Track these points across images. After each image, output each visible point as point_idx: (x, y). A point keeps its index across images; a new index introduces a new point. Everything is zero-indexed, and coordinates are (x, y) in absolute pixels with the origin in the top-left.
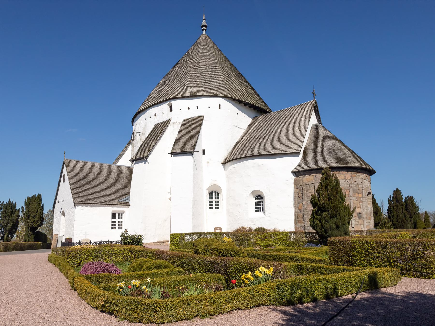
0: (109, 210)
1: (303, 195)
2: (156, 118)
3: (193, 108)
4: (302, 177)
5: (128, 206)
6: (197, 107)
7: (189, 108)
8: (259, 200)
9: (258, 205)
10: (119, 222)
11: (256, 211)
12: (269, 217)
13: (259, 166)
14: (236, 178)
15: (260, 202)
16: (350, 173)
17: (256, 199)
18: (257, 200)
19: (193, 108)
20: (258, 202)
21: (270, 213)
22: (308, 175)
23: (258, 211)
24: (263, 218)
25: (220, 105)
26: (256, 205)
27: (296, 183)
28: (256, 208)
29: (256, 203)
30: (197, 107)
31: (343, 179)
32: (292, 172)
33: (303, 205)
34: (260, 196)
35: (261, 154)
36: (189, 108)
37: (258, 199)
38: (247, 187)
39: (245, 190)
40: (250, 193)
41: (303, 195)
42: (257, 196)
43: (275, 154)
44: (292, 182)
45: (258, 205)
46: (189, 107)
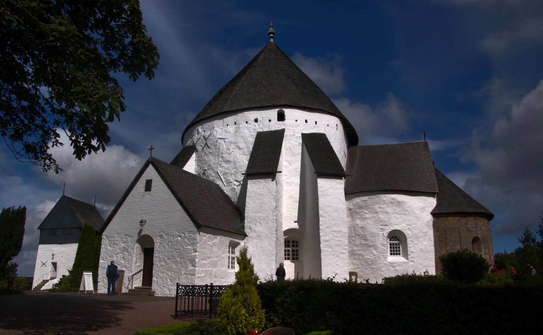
0: (227, 240)
1: (446, 239)
2: (258, 124)
3: (311, 123)
4: (444, 220)
5: (244, 236)
6: (316, 123)
7: (306, 121)
8: (395, 242)
9: (394, 248)
10: (232, 257)
11: (391, 254)
12: (413, 261)
13: (399, 202)
14: (367, 213)
15: (396, 244)
16: (486, 220)
17: (390, 240)
18: (392, 242)
19: (311, 123)
20: (393, 244)
21: (413, 258)
22: (450, 218)
23: (394, 254)
24: (406, 262)
25: (337, 125)
26: (391, 248)
27: (436, 227)
28: (391, 251)
29: (390, 244)
30: (316, 123)
31: (483, 226)
32: (431, 213)
33: (447, 249)
34: (396, 237)
35: (402, 189)
36: (306, 121)
37: (393, 240)
38: (385, 225)
39: (381, 228)
40: (388, 232)
41: (446, 239)
42: (393, 237)
43: (416, 192)
44: (431, 223)
45: (394, 248)
46: (306, 119)
